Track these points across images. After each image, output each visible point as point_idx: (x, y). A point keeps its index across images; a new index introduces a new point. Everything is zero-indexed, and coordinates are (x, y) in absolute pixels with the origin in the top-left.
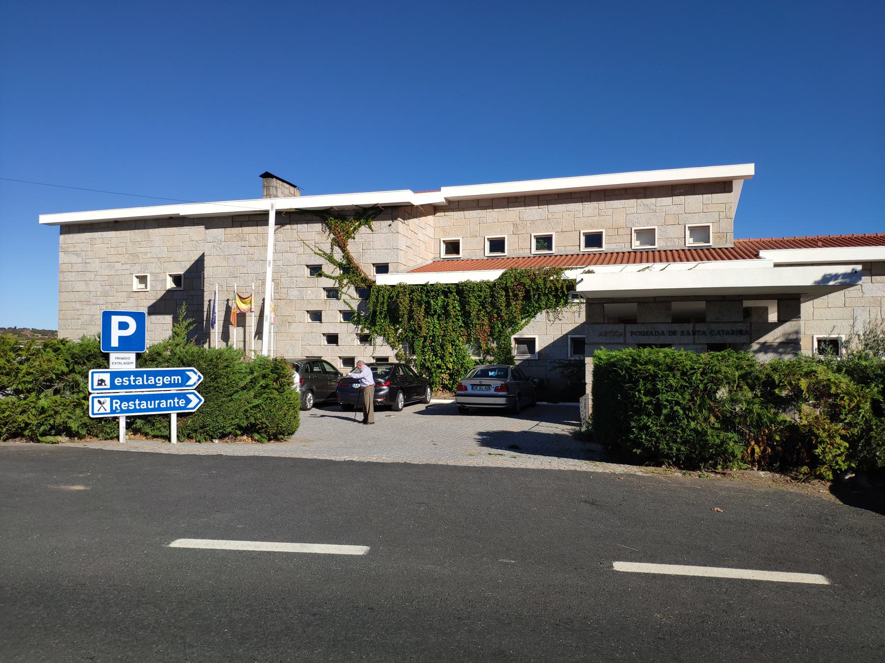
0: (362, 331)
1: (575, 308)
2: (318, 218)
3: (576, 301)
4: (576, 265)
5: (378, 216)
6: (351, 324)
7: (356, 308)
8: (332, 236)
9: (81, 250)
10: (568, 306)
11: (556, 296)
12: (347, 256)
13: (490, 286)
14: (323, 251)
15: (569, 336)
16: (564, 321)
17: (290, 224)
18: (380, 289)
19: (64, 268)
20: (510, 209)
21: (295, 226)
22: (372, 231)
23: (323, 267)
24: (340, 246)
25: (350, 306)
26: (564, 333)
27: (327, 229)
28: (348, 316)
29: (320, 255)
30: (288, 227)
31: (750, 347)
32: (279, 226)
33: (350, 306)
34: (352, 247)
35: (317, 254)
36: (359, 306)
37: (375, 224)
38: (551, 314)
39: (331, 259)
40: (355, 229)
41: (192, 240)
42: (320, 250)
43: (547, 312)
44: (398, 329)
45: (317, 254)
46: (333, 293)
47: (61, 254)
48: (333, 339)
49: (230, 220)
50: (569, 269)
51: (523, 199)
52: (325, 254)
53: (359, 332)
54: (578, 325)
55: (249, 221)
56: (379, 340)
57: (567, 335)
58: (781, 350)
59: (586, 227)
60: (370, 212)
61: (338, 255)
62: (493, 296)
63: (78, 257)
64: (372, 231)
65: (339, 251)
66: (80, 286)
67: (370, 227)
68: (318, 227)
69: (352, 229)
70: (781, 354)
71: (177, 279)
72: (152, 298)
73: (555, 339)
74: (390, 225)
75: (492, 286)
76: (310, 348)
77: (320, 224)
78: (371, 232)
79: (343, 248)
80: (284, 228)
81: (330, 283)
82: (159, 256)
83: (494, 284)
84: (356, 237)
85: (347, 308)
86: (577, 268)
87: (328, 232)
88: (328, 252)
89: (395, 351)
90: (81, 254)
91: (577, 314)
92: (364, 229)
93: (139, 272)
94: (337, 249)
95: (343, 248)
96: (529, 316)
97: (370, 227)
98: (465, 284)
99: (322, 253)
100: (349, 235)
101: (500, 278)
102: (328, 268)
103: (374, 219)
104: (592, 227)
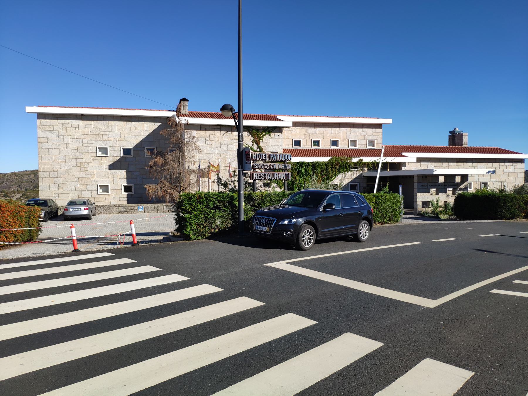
1: (352, 173)
5: (274, 131)
8: (252, 138)
9: (56, 130)
10: (349, 172)
11: (346, 168)
12: (259, 147)
13: (326, 164)
15: (350, 183)
16: (348, 177)
17: (231, 131)
19: (42, 140)
20: (303, 128)
22: (271, 137)
24: (256, 143)
26: (348, 182)
27: (250, 135)
30: (230, 132)
31: (457, 189)
32: (226, 132)
34: (262, 144)
37: (272, 134)
38: (343, 175)
40: (264, 135)
41: (138, 129)
42: (246, 144)
43: (342, 174)
47: (39, 132)
49: (199, 127)
50: (354, 158)
51: (308, 124)
54: (352, 179)
57: (349, 183)
58: (464, 190)
60: (270, 129)
62: (326, 168)
63: (53, 134)
64: (271, 137)
66: (57, 152)
67: (270, 136)
69: (262, 136)
70: (464, 191)
71: (127, 151)
74: (279, 135)
75: (327, 164)
77: (246, 133)
78: (270, 138)
79: (258, 144)
82: (115, 137)
83: (328, 163)
84: (263, 139)
86: (355, 158)
87: (250, 137)
90: (55, 132)
91: (352, 175)
92: (267, 136)
93: (101, 145)
94: (255, 145)
95: (258, 144)
96: (336, 175)
97: (270, 136)
99: (247, 146)
100: (261, 138)
101: (329, 160)
103: (272, 132)
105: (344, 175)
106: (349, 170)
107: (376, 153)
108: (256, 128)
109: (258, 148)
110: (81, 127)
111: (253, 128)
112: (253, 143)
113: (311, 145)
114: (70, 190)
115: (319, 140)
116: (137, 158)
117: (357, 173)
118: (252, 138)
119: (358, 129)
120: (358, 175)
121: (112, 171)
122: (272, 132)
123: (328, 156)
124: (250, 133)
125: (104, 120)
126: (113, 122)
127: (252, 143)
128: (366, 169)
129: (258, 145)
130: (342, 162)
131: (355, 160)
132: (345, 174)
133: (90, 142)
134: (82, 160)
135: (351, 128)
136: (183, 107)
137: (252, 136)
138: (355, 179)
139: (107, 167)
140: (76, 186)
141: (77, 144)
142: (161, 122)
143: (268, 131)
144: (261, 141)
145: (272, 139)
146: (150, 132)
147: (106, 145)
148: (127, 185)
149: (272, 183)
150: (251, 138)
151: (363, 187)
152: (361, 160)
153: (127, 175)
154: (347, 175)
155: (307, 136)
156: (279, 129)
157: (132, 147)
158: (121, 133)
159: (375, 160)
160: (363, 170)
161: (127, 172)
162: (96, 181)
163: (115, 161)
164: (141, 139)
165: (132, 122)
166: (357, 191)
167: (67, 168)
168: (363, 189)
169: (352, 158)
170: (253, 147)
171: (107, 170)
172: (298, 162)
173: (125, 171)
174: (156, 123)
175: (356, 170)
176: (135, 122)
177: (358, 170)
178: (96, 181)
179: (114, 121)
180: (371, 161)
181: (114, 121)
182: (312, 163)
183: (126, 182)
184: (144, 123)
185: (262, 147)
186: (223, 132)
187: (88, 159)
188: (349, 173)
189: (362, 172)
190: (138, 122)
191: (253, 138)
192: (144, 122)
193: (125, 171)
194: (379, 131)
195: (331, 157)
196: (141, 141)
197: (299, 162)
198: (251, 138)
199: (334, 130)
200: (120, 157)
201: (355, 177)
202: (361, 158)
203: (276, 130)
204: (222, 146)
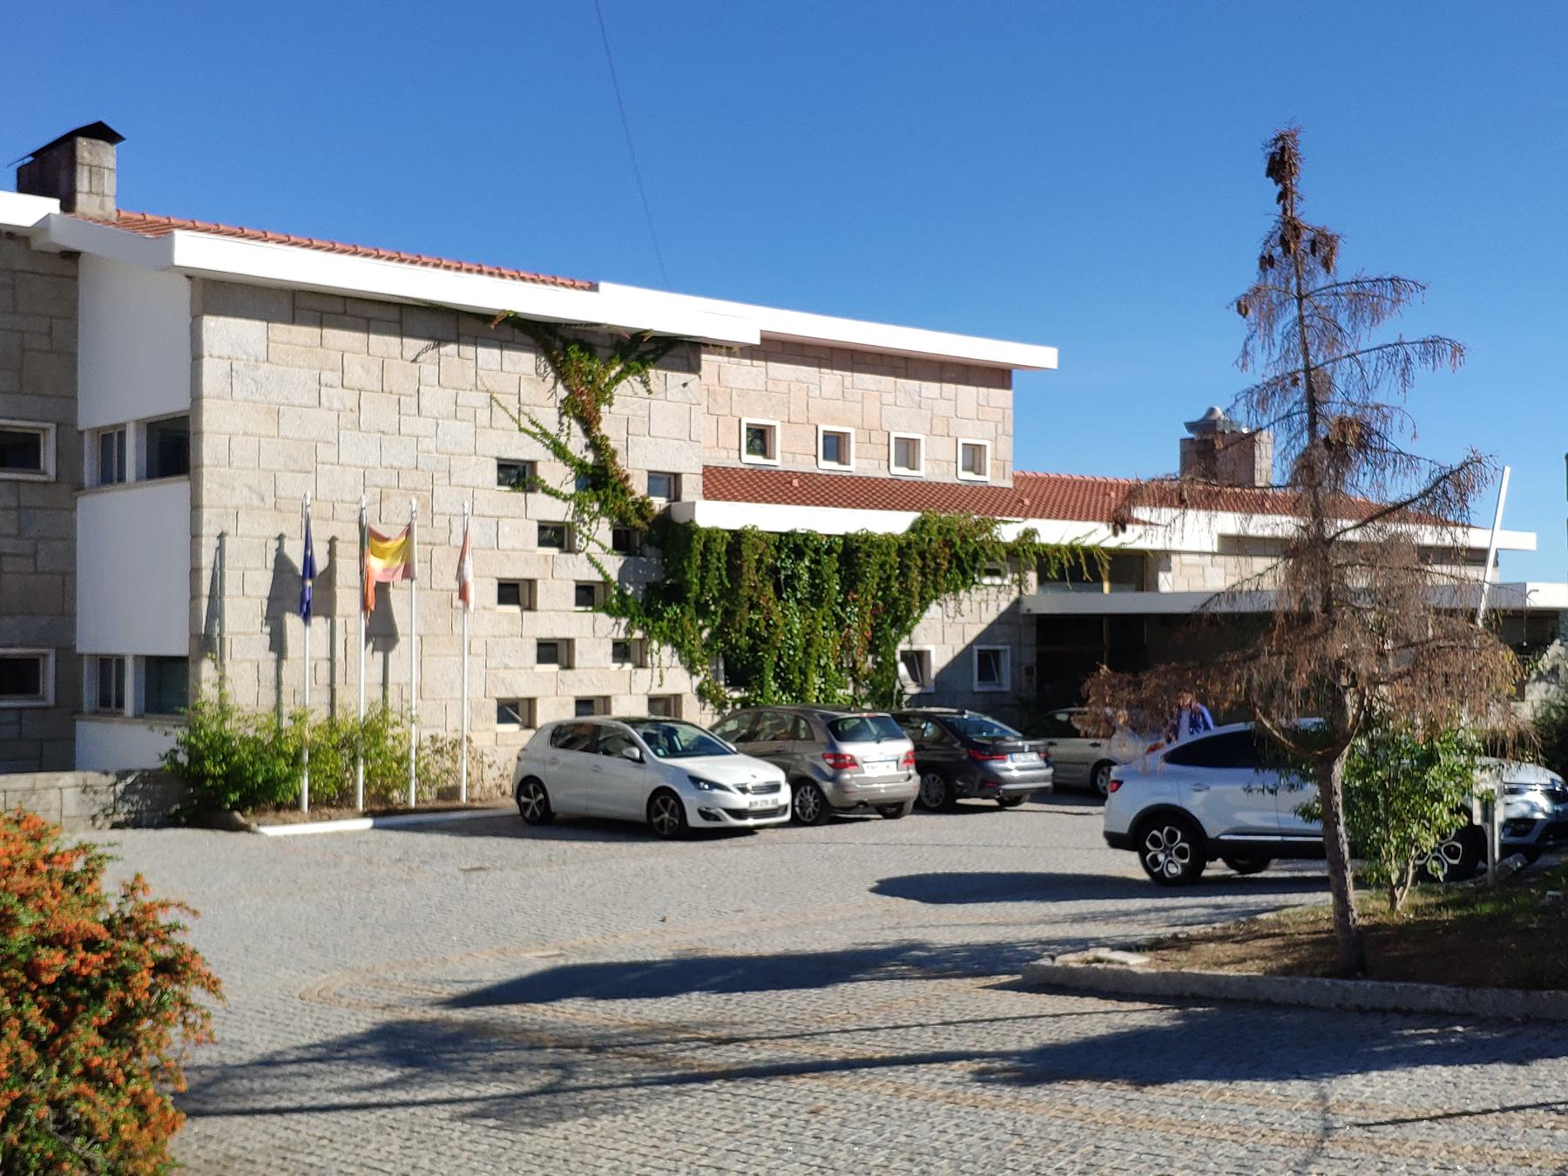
0: (628, 630)
2: (529, 340)
3: (987, 580)
4: (1001, 515)
5: (665, 359)
6: (602, 617)
7: (614, 577)
8: (562, 393)
12: (597, 445)
14: (541, 428)
15: (976, 648)
18: (711, 535)
21: (468, 351)
23: (540, 467)
25: (600, 570)
26: (968, 640)
27: (549, 369)
28: (586, 594)
29: (534, 436)
33: (600, 570)
34: (610, 424)
35: (527, 431)
36: (622, 572)
39: (560, 452)
42: (533, 423)
44: (701, 629)
45: (527, 431)
46: (555, 536)
48: (553, 651)
52: (545, 434)
53: (622, 635)
55: (345, 313)
56: (665, 655)
59: (825, 422)
61: (576, 443)
65: (576, 429)
67: (645, 383)
68: (524, 362)
73: (956, 653)
75: (903, 548)
76: (507, 675)
77: (532, 356)
79: (588, 423)
80: (443, 350)
81: (558, 511)
85: (595, 576)
88: (553, 429)
89: (697, 681)
91: (983, 605)
95: (588, 423)
98: (867, 538)
99: (537, 430)
100: (602, 395)
101: (913, 529)
102: (555, 474)
104: (834, 421)
105: (952, 604)
106: (974, 583)
107: (1027, 502)
108: (580, 336)
109: (587, 447)
111: (568, 334)
112: (565, 419)
113: (740, 450)
115: (772, 428)
117: (1001, 596)
118: (560, 387)
119: (925, 384)
120: (1004, 606)
122: (654, 360)
123: (911, 509)
124: (552, 361)
127: (561, 416)
128: (1032, 577)
129: (587, 432)
130: (964, 539)
131: (1008, 532)
132: (960, 602)
135: (897, 376)
137: (561, 375)
138: (992, 626)
143: (634, 356)
144: (604, 408)
145: (653, 402)
149: (655, 644)
150: (554, 387)
151: (1023, 668)
152: (1030, 534)
154: (965, 606)
155: (720, 400)
156: (682, 351)
159: (1077, 538)
160: (1021, 583)
166: (1000, 685)
168: (1023, 672)
169: (997, 522)
170: (563, 440)
172: (781, 534)
175: (997, 581)
177: (1006, 582)
180: (1065, 542)
182: (845, 537)
185: (612, 444)
186: (414, 345)
188: (977, 595)
189: (1021, 592)
191: (567, 388)
194: (1001, 398)
195: (917, 515)
197: (787, 534)
198: (554, 387)
199: (832, 380)
201: (990, 616)
202: (1032, 523)
203: (670, 353)
204: (411, 424)
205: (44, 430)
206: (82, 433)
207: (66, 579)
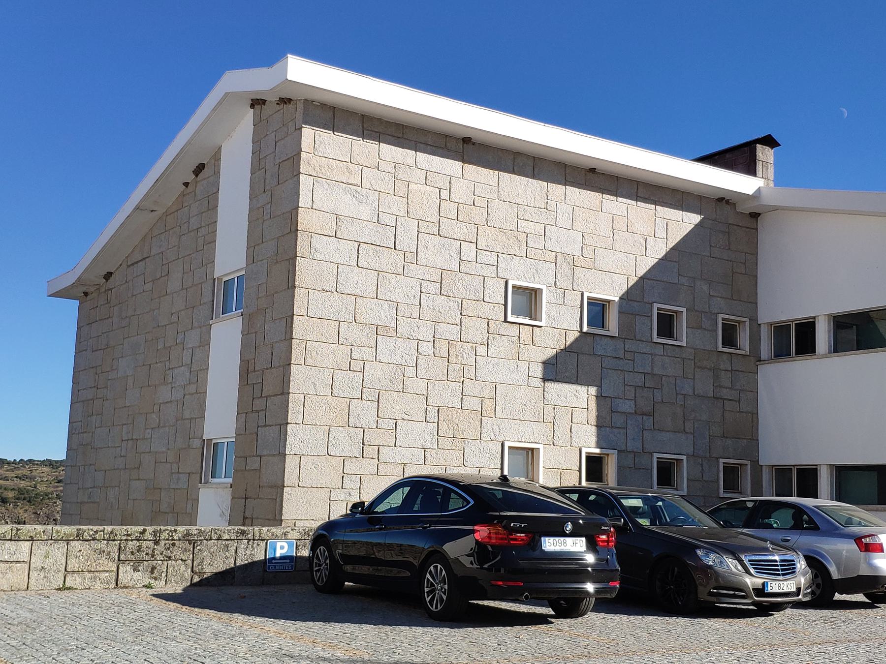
72: (550, 344)
110: (461, 192)
114: (407, 461)
116: (629, 345)
121: (554, 388)
125: (533, 176)
126: (560, 188)
133: (484, 257)
134: (452, 332)
136: (761, 167)
139: (538, 371)
140: (428, 445)
141: (441, 264)
142: (700, 214)
146: (671, 245)
147: (537, 279)
148: (597, 451)
153: (598, 410)
157: (617, 299)
158: (585, 235)
161: (599, 397)
162: (496, 427)
163: (563, 347)
164: (641, 272)
165: (620, 199)
167: (400, 362)
171: (538, 383)
173: (593, 390)
174: (689, 214)
176: (629, 201)
178: (496, 427)
179: (566, 183)
181: (565, 185)
183: (593, 439)
184: (653, 206)
187: (475, 331)
190: (634, 202)
192: (655, 203)
193: (593, 390)
196: (642, 278)
200: (577, 334)
205: (739, 322)
206: (760, 325)
207: (754, 415)
